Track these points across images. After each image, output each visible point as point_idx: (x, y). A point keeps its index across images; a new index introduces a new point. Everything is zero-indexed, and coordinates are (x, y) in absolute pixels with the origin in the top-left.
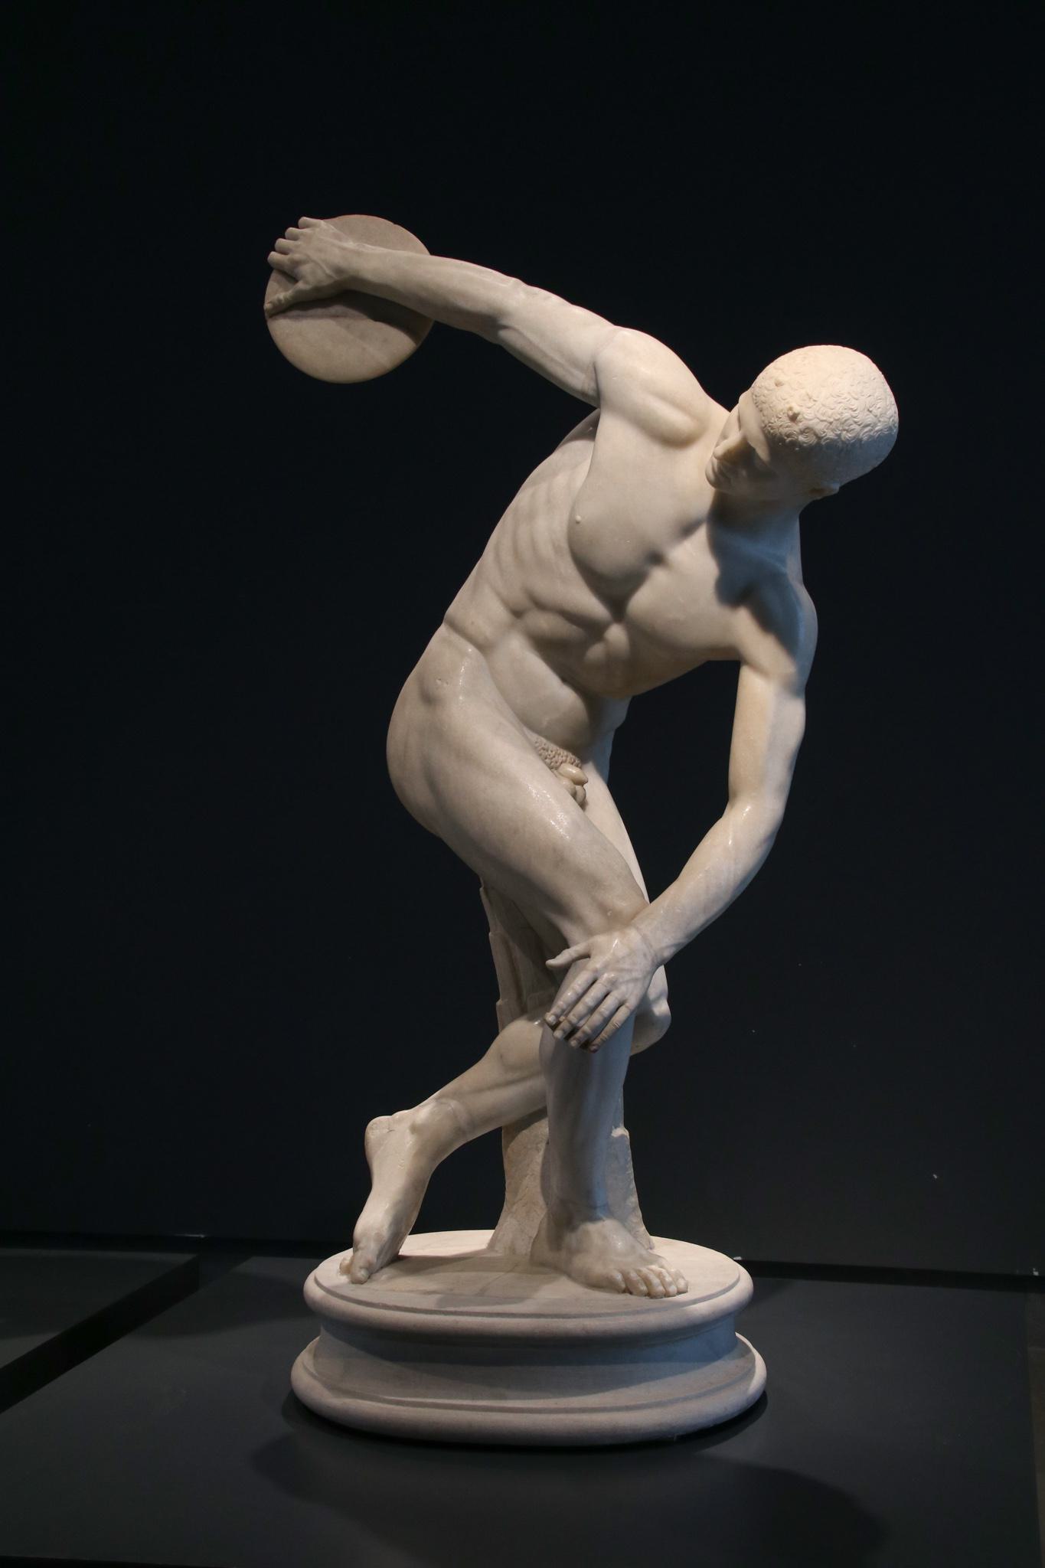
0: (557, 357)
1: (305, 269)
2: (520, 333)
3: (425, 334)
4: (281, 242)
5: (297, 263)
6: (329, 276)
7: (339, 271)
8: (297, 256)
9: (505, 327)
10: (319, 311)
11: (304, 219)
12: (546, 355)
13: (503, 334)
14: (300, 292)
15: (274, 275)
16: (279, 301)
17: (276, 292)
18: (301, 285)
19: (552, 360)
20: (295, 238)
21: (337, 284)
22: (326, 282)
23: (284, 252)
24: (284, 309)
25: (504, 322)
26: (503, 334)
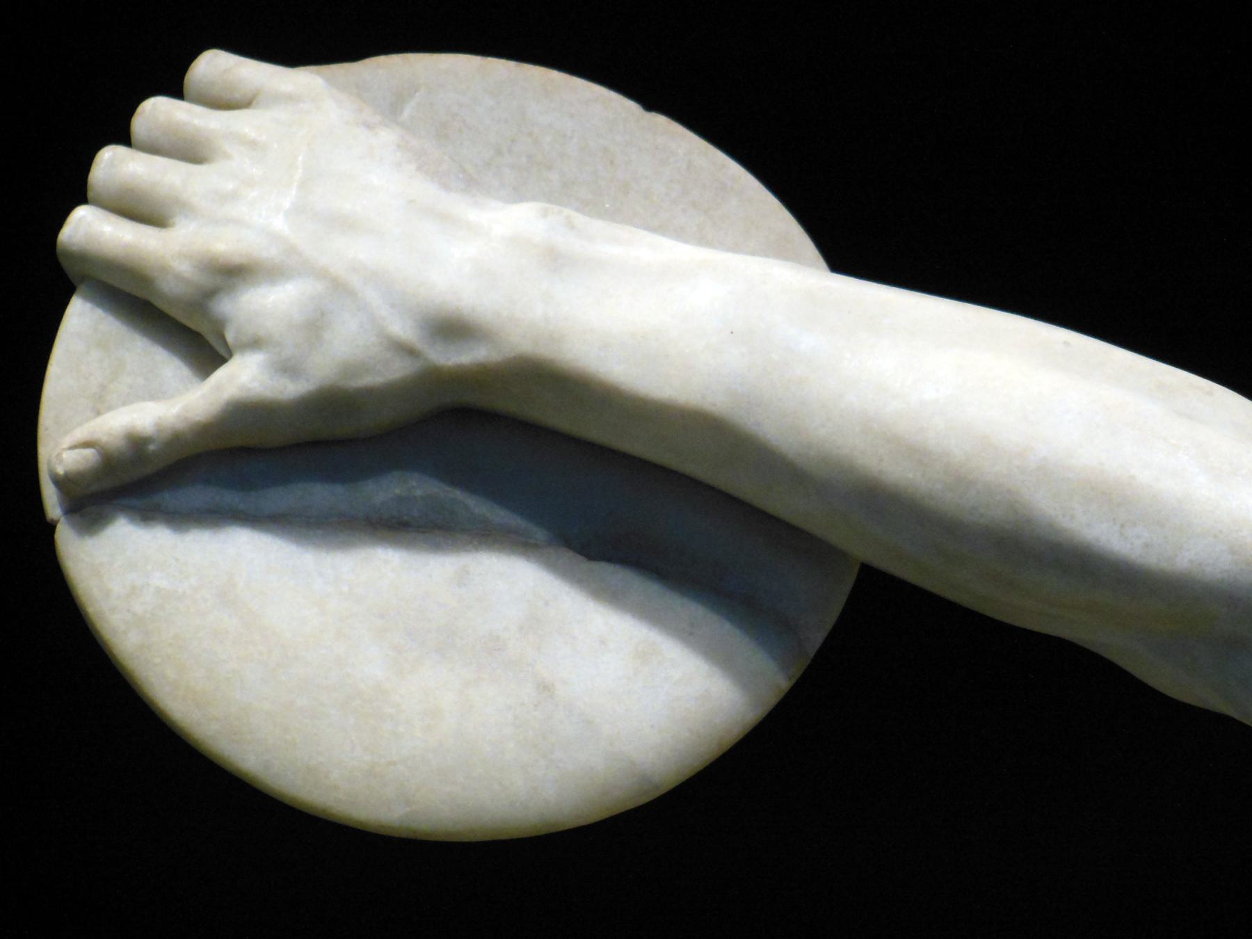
1: (262, 306)
3: (816, 638)
4: (113, 165)
5: (233, 274)
6: (408, 351)
7: (452, 328)
8: (226, 243)
10: (321, 494)
11: (214, 66)
15: (82, 323)
16: (137, 443)
17: (101, 392)
18: (243, 377)
20: (189, 151)
21: (434, 379)
22: (398, 370)
23: (141, 210)
24: (148, 481)
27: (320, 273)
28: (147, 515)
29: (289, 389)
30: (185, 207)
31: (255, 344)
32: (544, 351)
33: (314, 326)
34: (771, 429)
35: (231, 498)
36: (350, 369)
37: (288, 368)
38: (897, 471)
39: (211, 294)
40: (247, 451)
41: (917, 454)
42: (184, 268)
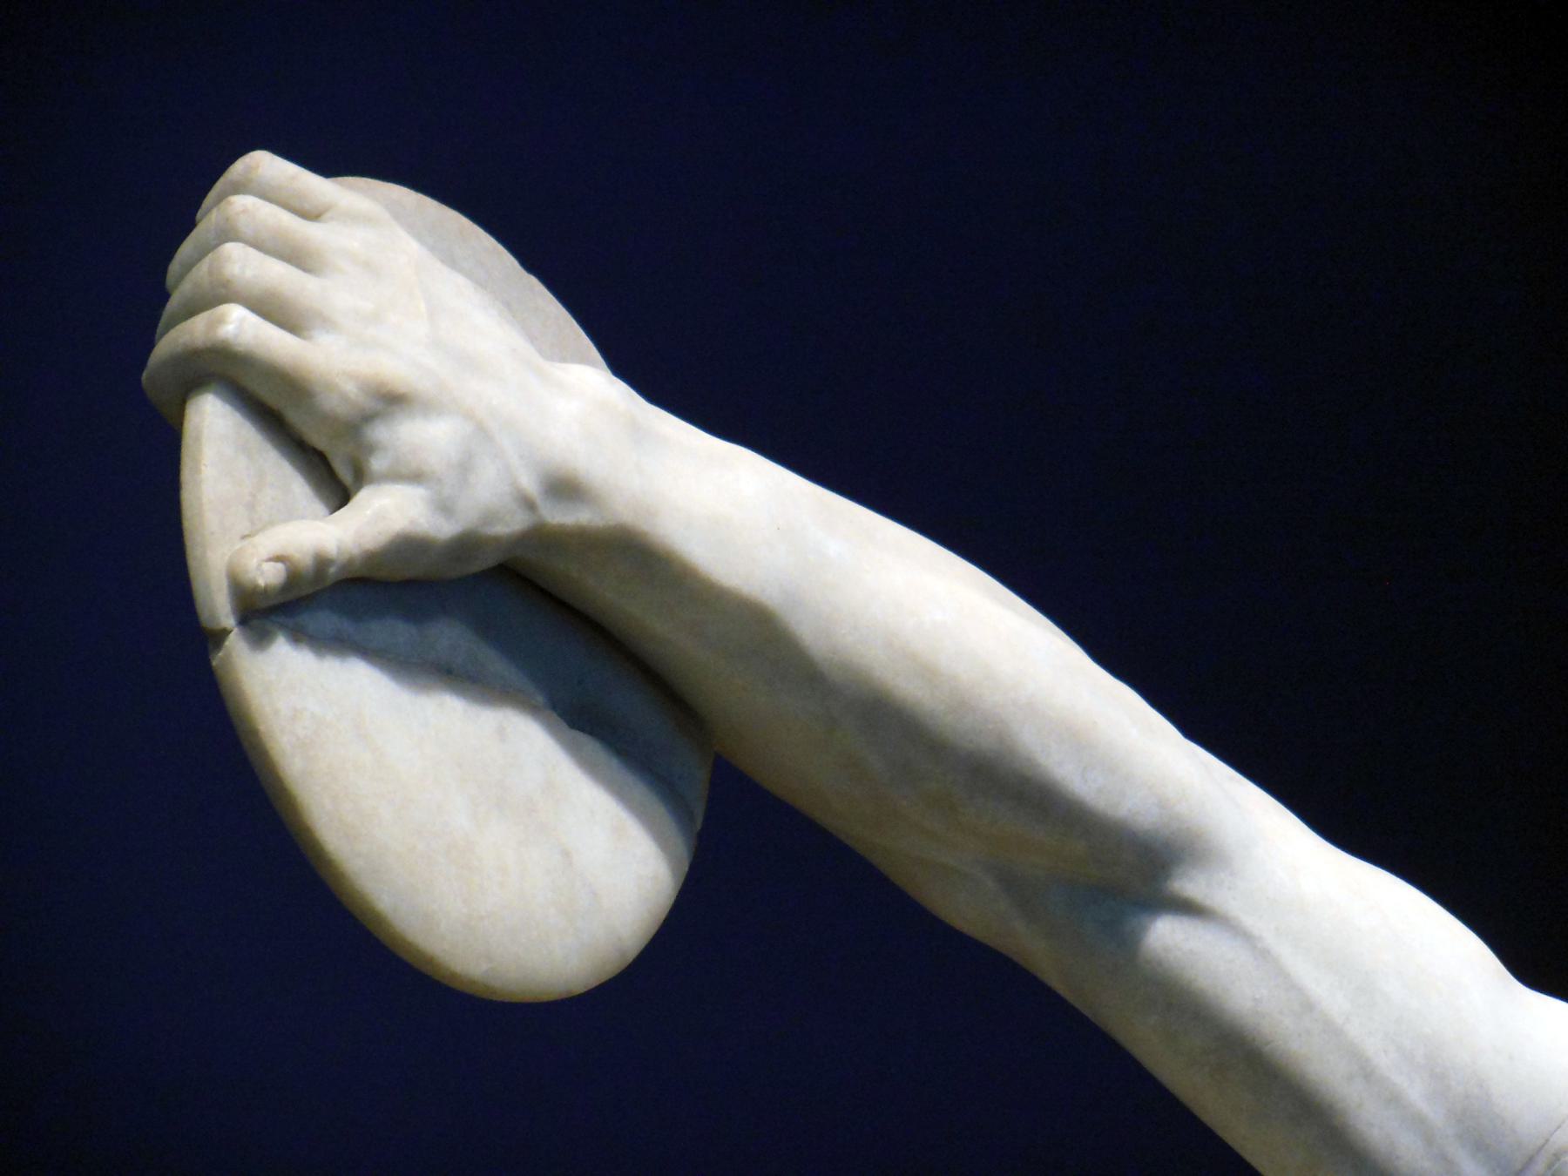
0: (1415, 1092)
2: (1263, 954)
5: (391, 401)
6: (529, 504)
7: (564, 488)
9: (1188, 908)
10: (398, 631)
12: (1367, 1072)
13: (1166, 936)
14: (407, 547)
16: (322, 563)
19: (1394, 1099)
21: (542, 538)
22: (513, 523)
25: (1190, 885)
26: (1166, 936)
27: (469, 415)
28: (299, 636)
29: (443, 529)
30: (327, 323)
31: (415, 477)
32: (643, 524)
33: (465, 467)
34: (806, 630)
35: (346, 626)
36: (490, 517)
37: (444, 507)
38: (907, 688)
39: (369, 418)
40: (409, 584)
41: (928, 673)
42: (350, 388)
